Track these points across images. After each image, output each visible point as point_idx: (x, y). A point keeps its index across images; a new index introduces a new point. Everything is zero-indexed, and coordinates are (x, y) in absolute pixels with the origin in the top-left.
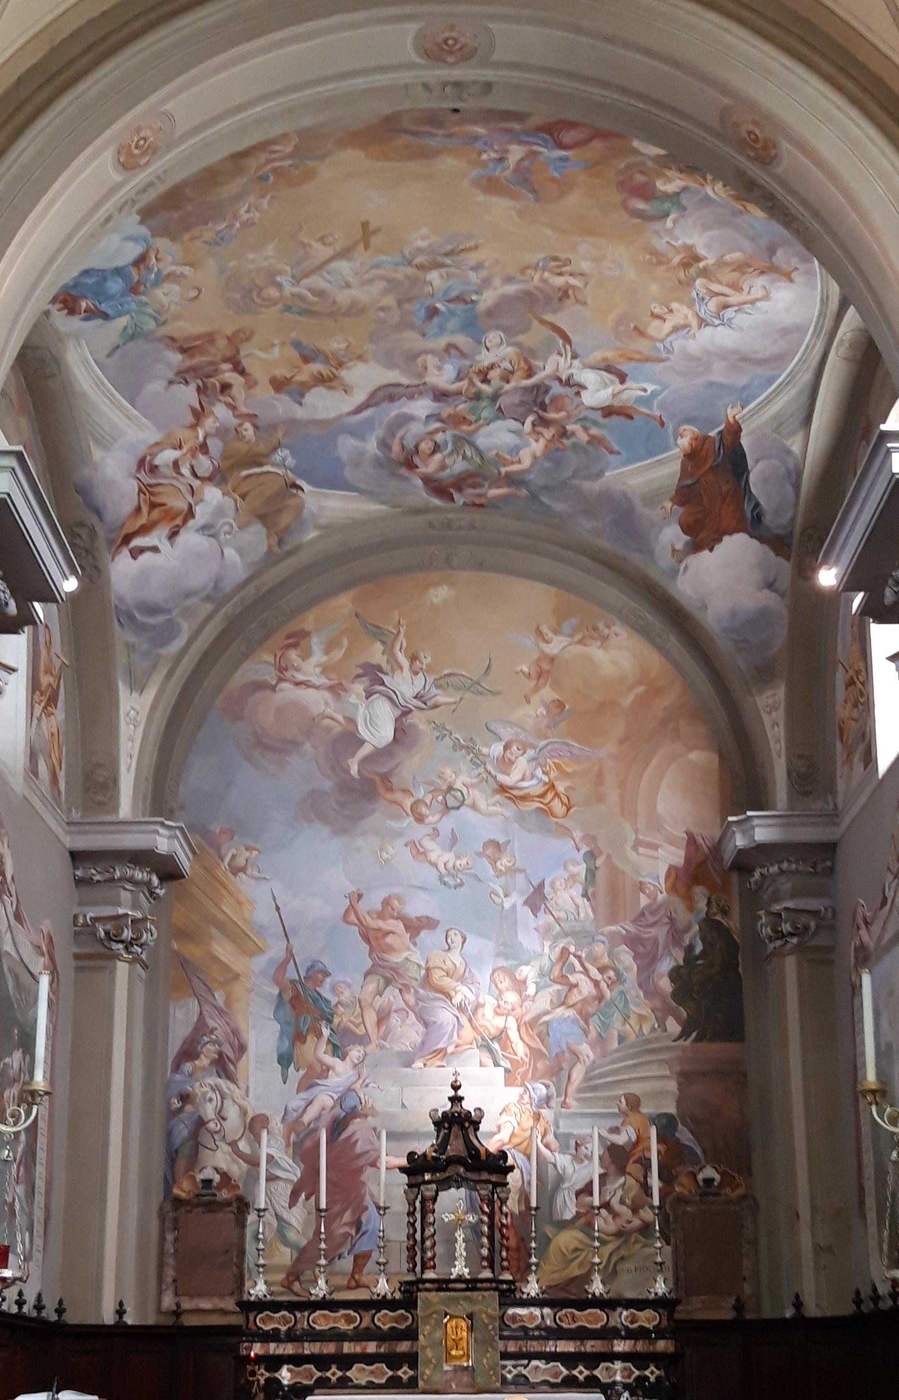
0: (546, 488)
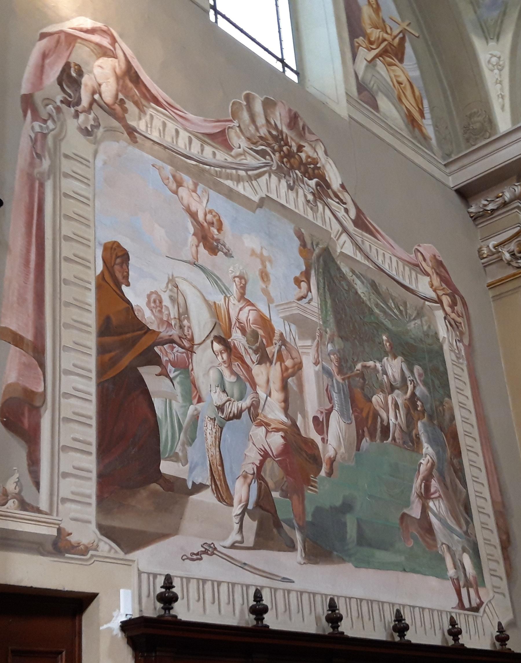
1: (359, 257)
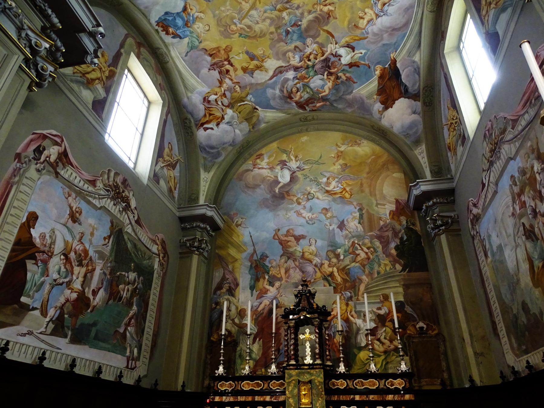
0: (335, 100)
1: (133, 234)
